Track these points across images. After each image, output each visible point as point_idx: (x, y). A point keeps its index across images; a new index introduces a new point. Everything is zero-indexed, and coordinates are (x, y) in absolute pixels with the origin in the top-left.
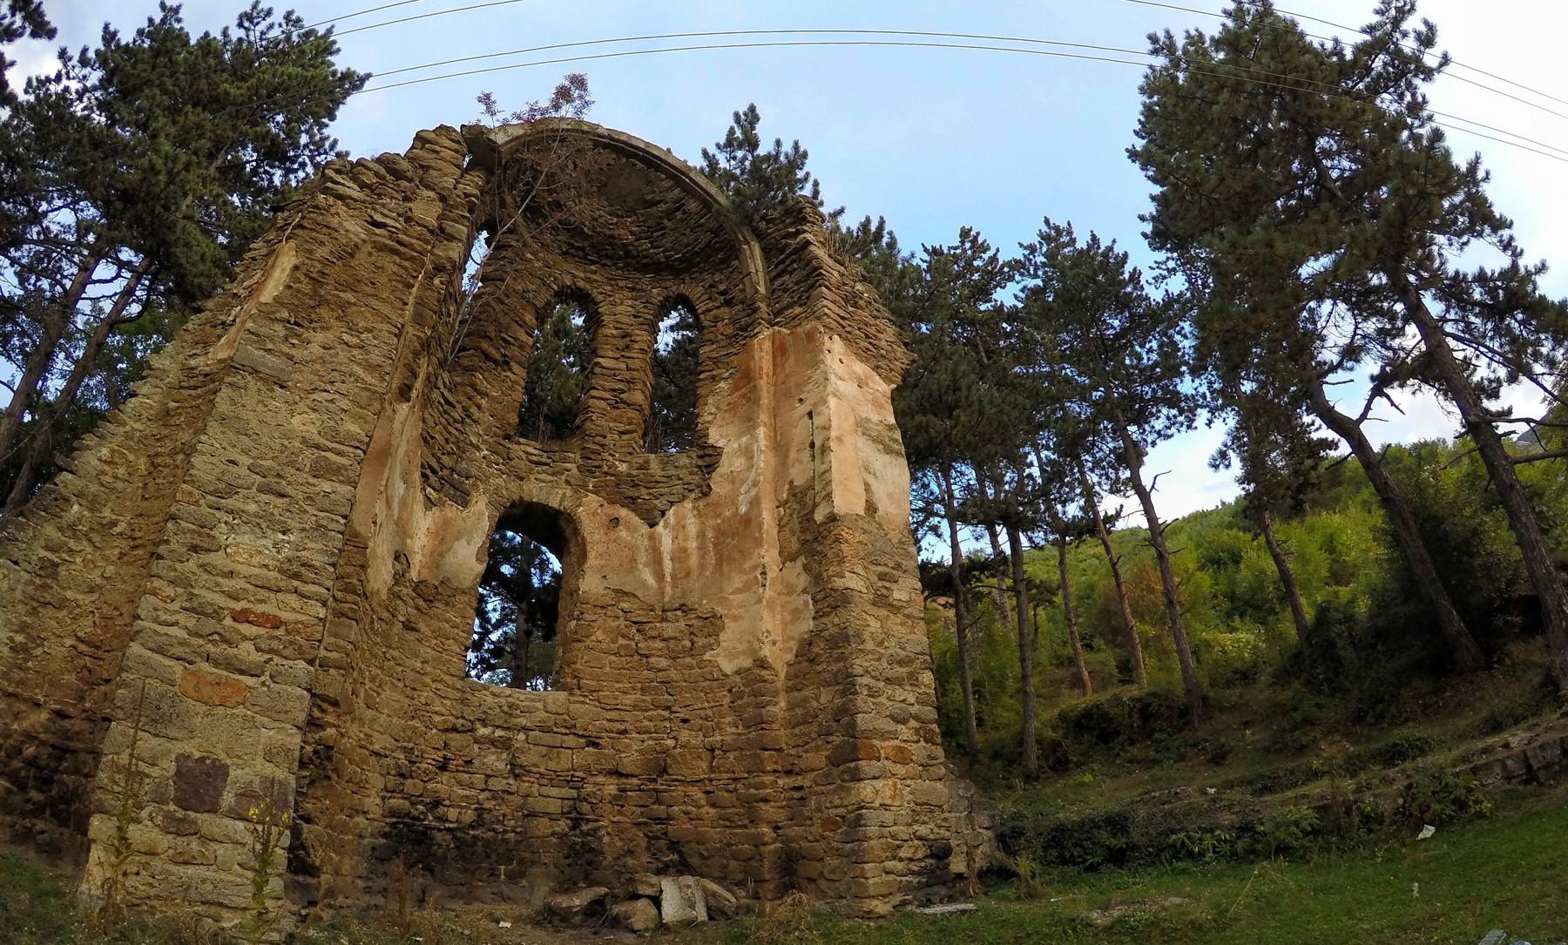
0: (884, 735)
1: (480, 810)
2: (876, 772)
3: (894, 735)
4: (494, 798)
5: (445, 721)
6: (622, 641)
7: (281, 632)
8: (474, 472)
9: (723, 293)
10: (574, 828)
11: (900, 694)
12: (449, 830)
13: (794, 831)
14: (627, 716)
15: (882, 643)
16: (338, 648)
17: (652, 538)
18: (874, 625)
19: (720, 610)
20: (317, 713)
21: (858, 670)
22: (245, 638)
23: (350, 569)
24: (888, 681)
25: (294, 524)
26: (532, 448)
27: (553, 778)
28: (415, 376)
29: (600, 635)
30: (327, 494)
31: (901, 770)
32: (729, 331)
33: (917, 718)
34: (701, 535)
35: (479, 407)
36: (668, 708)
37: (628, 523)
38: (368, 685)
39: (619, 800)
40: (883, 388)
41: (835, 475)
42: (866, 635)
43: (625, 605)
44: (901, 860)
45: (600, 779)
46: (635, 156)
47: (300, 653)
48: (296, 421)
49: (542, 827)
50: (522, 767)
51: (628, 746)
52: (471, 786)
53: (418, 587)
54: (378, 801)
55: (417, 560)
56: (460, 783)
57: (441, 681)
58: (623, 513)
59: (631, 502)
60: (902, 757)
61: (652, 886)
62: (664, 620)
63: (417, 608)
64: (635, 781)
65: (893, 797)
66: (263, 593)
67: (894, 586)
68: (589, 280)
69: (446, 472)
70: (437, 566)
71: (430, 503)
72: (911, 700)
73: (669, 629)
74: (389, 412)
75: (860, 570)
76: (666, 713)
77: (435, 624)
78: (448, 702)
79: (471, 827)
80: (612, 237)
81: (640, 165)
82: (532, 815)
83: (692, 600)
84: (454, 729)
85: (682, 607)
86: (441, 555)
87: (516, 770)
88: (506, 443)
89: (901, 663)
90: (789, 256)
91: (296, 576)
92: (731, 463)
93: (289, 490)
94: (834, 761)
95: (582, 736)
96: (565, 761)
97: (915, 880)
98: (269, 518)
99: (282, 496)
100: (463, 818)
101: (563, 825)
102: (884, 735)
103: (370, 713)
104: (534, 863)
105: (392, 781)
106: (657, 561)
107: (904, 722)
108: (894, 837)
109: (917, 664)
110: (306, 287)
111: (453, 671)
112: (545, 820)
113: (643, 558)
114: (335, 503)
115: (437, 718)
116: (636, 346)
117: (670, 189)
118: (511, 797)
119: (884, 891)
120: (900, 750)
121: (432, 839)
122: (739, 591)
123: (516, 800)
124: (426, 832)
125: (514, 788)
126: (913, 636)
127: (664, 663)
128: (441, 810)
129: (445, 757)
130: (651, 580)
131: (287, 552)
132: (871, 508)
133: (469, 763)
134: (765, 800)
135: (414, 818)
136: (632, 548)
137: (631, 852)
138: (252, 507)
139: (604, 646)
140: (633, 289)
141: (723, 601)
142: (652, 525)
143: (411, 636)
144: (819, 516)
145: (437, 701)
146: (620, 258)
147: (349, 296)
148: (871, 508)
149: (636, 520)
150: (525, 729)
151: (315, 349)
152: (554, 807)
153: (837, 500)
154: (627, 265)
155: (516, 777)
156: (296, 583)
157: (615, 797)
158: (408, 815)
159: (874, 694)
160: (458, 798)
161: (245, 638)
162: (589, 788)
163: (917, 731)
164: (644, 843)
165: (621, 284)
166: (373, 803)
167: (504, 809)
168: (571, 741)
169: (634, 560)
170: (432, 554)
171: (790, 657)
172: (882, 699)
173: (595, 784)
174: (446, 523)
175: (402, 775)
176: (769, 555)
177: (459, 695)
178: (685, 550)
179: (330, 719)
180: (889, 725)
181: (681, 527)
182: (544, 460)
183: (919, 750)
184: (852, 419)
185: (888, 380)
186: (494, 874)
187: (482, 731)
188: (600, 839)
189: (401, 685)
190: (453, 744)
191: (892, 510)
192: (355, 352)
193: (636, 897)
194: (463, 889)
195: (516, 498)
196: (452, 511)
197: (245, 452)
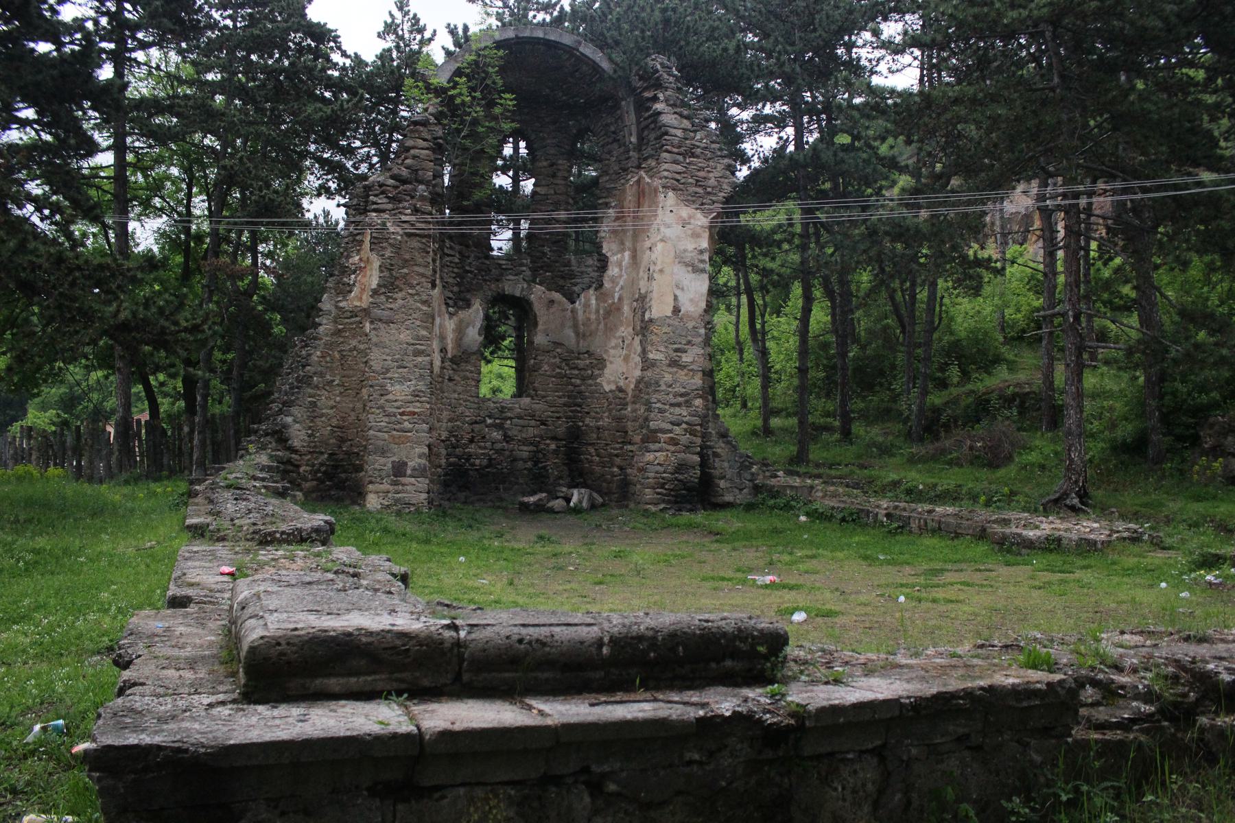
1: (490, 460)
3: (671, 431)
9: (614, 133)
11: (677, 410)
13: (629, 471)
19: (605, 356)
24: (672, 405)
27: (525, 442)
29: (546, 367)
31: (672, 448)
32: (616, 168)
33: (686, 423)
34: (597, 311)
36: (580, 406)
39: (555, 452)
40: (701, 220)
41: (655, 295)
42: (661, 383)
47: (424, 421)
52: (485, 448)
53: (451, 360)
55: (450, 347)
56: (480, 447)
58: (557, 296)
59: (560, 289)
60: (673, 441)
67: (684, 355)
71: (451, 315)
73: (581, 363)
82: (515, 460)
83: (592, 349)
84: (476, 422)
85: (587, 352)
87: (508, 439)
89: (682, 395)
90: (650, 116)
92: (613, 271)
94: (643, 441)
96: (531, 432)
98: (403, 377)
101: (529, 464)
107: (678, 425)
110: (386, 274)
116: (559, 174)
120: (672, 439)
122: (613, 348)
123: (507, 453)
127: (578, 382)
134: (617, 456)
137: (561, 478)
141: (606, 351)
142: (573, 302)
144: (647, 317)
147: (405, 271)
148: (676, 310)
150: (511, 418)
152: (525, 455)
153: (653, 311)
159: (661, 411)
163: (685, 430)
166: (443, 461)
168: (533, 423)
171: (632, 386)
174: (461, 321)
176: (625, 331)
178: (589, 319)
180: (669, 427)
181: (587, 305)
184: (672, 254)
185: (706, 213)
186: (497, 489)
187: (489, 421)
191: (692, 309)
193: (558, 498)
196: (462, 314)
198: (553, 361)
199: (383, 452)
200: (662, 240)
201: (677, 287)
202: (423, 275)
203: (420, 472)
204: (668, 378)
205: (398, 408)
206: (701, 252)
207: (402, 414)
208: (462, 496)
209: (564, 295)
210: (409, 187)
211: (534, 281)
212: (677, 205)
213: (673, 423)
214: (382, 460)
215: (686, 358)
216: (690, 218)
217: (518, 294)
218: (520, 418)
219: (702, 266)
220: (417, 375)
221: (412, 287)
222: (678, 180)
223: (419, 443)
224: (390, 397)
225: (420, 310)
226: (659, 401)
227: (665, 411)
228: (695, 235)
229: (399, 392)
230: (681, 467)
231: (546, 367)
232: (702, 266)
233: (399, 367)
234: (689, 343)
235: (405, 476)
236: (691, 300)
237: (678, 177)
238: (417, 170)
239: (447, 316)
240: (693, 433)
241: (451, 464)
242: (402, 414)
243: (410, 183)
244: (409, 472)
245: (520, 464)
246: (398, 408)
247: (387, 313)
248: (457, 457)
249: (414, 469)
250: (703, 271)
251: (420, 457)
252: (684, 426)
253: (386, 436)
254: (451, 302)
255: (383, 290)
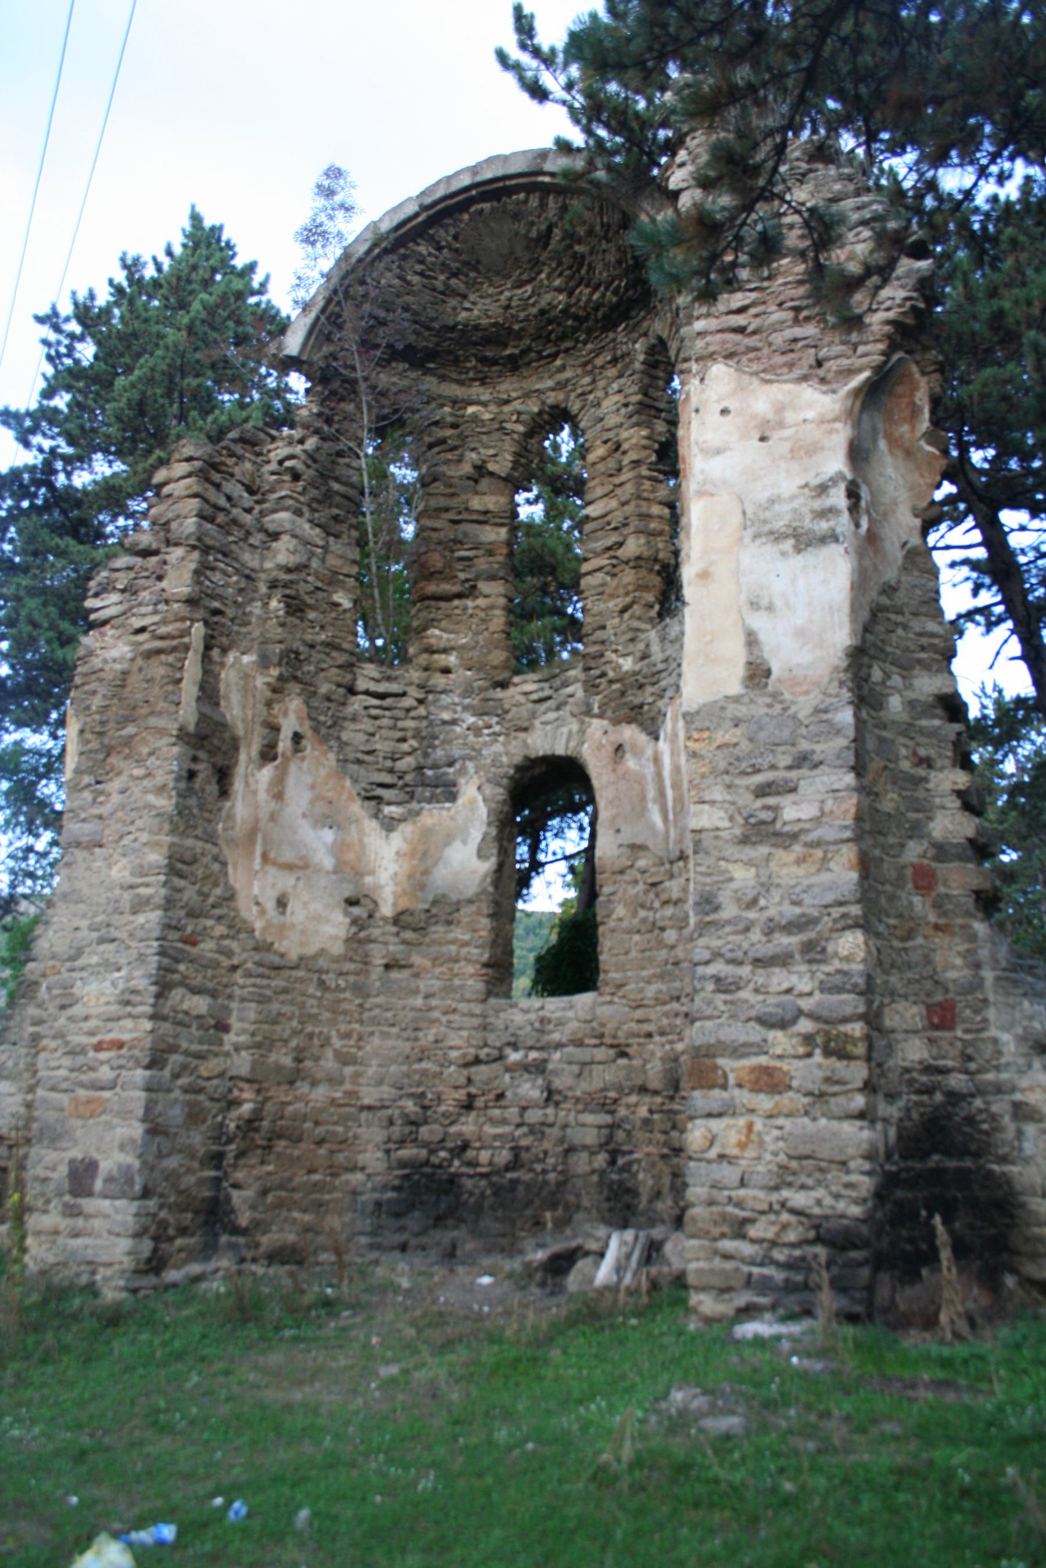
0: (738, 1051)
1: (516, 1150)
2: (715, 1107)
3: (761, 1048)
4: (532, 1132)
5: (464, 1055)
6: (642, 913)
7: (124, 1051)
8: (457, 753)
10: (612, 1162)
11: (779, 979)
12: (483, 1175)
14: (653, 1014)
15: (754, 902)
16: (244, 1031)
17: (657, 760)
18: (743, 876)
20: (236, 1093)
21: (706, 955)
22: (102, 1063)
23: (245, 956)
24: (758, 962)
25: (123, 961)
26: (528, 684)
28: (276, 729)
30: (142, 927)
31: (765, 1102)
33: (811, 1016)
35: (446, 671)
37: (634, 746)
38: (337, 1043)
42: (724, 897)
43: (641, 863)
44: (753, 1241)
45: (633, 1099)
46: (471, 201)
48: (114, 873)
49: (581, 1163)
50: (560, 1092)
51: (653, 1053)
52: (504, 1122)
53: (396, 921)
54: (380, 1154)
57: (455, 1011)
58: (630, 733)
60: (769, 1081)
61: (598, 1239)
62: (672, 876)
63: (405, 942)
64: (659, 1100)
65: (742, 1146)
66: (110, 1025)
68: (560, 386)
69: (409, 778)
70: (422, 887)
71: (390, 825)
72: (804, 985)
74: (253, 786)
75: (718, 794)
76: (675, 1005)
77: (435, 949)
78: (465, 1033)
79: (507, 1168)
80: (542, 312)
81: (486, 206)
82: (570, 1150)
84: (477, 1061)
86: (426, 872)
87: (551, 1096)
88: (499, 693)
89: (791, 927)
91: (128, 1003)
93: (116, 934)
95: (612, 1046)
97: (779, 1276)
99: (113, 940)
100: (496, 1160)
101: (601, 1160)
102: (738, 1051)
103: (348, 1070)
104: (578, 1207)
105: (397, 1131)
106: (662, 794)
107: (783, 1024)
108: (739, 1205)
109: (826, 922)
111: (468, 996)
112: (584, 1156)
113: (651, 793)
114: (150, 931)
115: (454, 1054)
117: (543, 205)
118: (548, 1130)
119: (718, 1282)
120: (766, 1071)
121: (460, 1187)
123: (554, 1132)
124: (453, 1180)
125: (551, 1119)
126: (825, 877)
128: (470, 1154)
129: (469, 1095)
130: (659, 823)
131: (121, 986)
132: (758, 674)
133: (501, 1096)
135: (434, 1166)
136: (640, 779)
138: (95, 959)
139: (625, 924)
140: (614, 361)
142: (657, 739)
143: (395, 975)
145: (453, 1035)
146: (575, 330)
147: (130, 730)
148: (758, 674)
149: (642, 738)
150: (559, 1046)
151: (116, 798)
152: (591, 1137)
154: (589, 332)
155: (557, 1104)
156: (129, 1009)
157: (646, 1122)
158: (427, 1163)
159: (722, 985)
160: (490, 1138)
161: (102, 1063)
162: (622, 1112)
163: (808, 1039)
164: (667, 1181)
165: (599, 362)
167: (546, 1145)
168: (602, 1053)
169: (643, 798)
170: (410, 877)
172: (745, 994)
173: (628, 1106)
175: (412, 1123)
177: (476, 1022)
179: (246, 1095)
182: (547, 692)
183: (809, 1071)
184: (736, 519)
186: (538, 1223)
187: (514, 1056)
188: (634, 1175)
189: (394, 1030)
190: (476, 1078)
192: (145, 782)
194: (504, 1242)
195: (518, 759)
196: (433, 815)
197: (84, 916)
198: (632, 891)
199: (54, 1137)
200: (701, 494)
201: (754, 605)
202: (162, 732)
203: (120, 1185)
204: (743, 876)
205: (92, 1034)
206: (823, 489)
207: (98, 1047)
208: (446, 1236)
209: (642, 726)
210: (154, 559)
211: (588, 712)
212: (741, 388)
213: (767, 1022)
214: (51, 1156)
215: (794, 811)
216: (780, 408)
217: (560, 751)
218: (579, 1043)
219: (824, 525)
220: (134, 954)
221: (140, 762)
222: (741, 330)
223: (124, 1114)
224: (77, 1010)
225: (149, 806)
226: (717, 955)
227: (737, 985)
228: (804, 451)
229: (97, 993)
230: (801, 1164)
231: (620, 911)
232: (824, 525)
233: (102, 941)
234: (802, 760)
235: (90, 1194)
236: (801, 634)
237: (739, 320)
238: (167, 523)
239: (371, 826)
240: (836, 1050)
241: (403, 1164)
242: (98, 1047)
243: (156, 553)
244: (98, 1185)
245: (581, 1163)
246: (92, 1034)
247: (88, 827)
248: (426, 1145)
249: (109, 1180)
250: (832, 537)
251: (122, 1147)
252: (805, 1026)
253: (65, 1099)
254: (380, 792)
255: (87, 779)
